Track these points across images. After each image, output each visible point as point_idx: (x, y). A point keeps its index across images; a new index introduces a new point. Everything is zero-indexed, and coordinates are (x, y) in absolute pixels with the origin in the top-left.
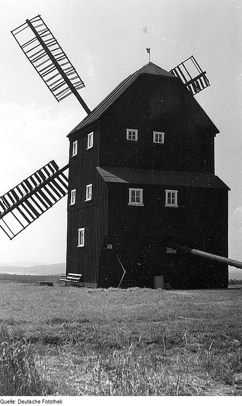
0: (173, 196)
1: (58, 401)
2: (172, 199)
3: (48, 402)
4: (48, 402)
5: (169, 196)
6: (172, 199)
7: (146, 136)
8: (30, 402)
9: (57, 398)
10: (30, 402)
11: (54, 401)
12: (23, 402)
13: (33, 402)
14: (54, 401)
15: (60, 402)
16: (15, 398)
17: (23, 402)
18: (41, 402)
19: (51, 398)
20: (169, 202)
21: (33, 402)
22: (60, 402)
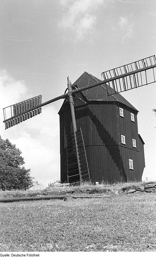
1: (37, 255)
4: (31, 255)
8: (19, 256)
9: (36, 253)
10: (19, 256)
11: (34, 255)
12: (14, 255)
13: (21, 256)
14: (34, 255)
15: (38, 255)
16: (9, 253)
17: (14, 255)
18: (26, 255)
19: (32, 253)
21: (21, 256)
22: (38, 255)
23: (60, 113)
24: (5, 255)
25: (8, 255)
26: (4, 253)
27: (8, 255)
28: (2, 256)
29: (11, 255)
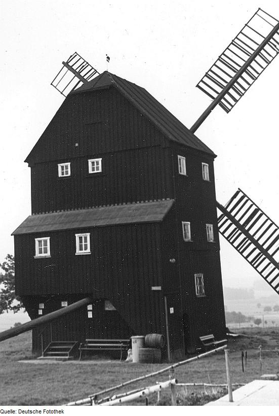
0: (86, 241)
1: (60, 411)
2: (83, 246)
3: (49, 412)
4: (49, 412)
5: (81, 242)
6: (83, 246)
8: (31, 412)
9: (58, 408)
10: (31, 412)
11: (55, 411)
12: (23, 412)
13: (34, 412)
14: (55, 411)
16: (15, 408)
17: (23, 412)
18: (42, 412)
19: (52, 408)
20: (81, 249)
21: (34, 412)
23: (30, 160)
24: (9, 411)
25: (13, 412)
27: (13, 412)
29: (17, 412)
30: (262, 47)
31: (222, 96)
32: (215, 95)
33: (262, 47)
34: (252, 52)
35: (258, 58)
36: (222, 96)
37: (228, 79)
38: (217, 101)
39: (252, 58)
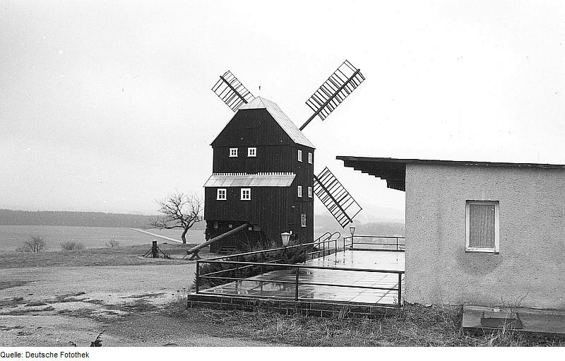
1: (83, 354)
3: (69, 355)
4: (69, 355)
7: (243, 152)
8: (43, 355)
9: (81, 350)
10: (43, 355)
11: (77, 355)
12: (32, 355)
13: (48, 355)
14: (77, 355)
15: (85, 355)
17: (32, 355)
18: (59, 354)
19: (73, 350)
21: (48, 355)
22: (85, 355)
24: (12, 354)
25: (18, 355)
26: (9, 350)
27: (18, 355)
28: (5, 356)
29: (24, 355)
30: (346, 84)
31: (320, 110)
32: (316, 110)
33: (346, 84)
34: (340, 86)
35: (343, 90)
36: (320, 110)
37: (325, 101)
38: (317, 113)
39: (340, 90)
